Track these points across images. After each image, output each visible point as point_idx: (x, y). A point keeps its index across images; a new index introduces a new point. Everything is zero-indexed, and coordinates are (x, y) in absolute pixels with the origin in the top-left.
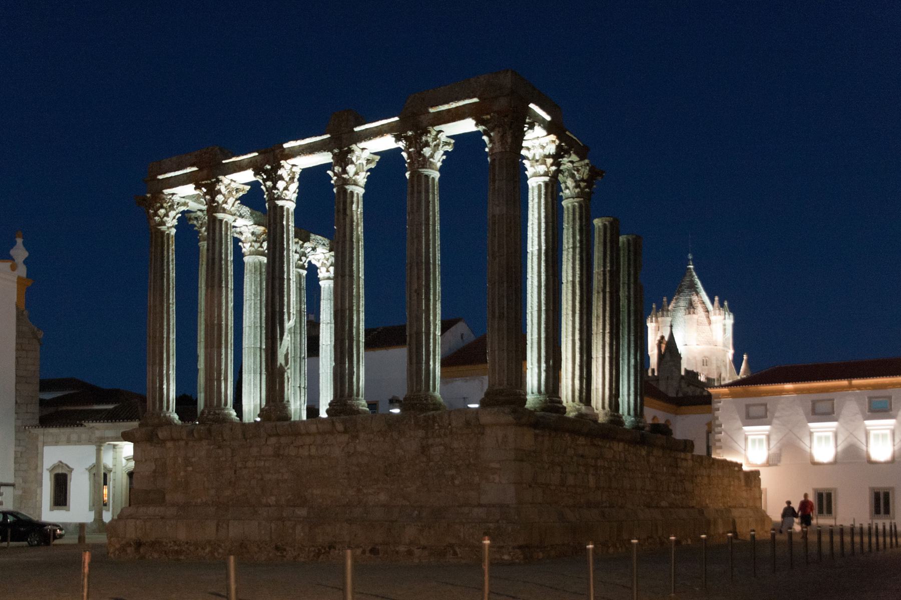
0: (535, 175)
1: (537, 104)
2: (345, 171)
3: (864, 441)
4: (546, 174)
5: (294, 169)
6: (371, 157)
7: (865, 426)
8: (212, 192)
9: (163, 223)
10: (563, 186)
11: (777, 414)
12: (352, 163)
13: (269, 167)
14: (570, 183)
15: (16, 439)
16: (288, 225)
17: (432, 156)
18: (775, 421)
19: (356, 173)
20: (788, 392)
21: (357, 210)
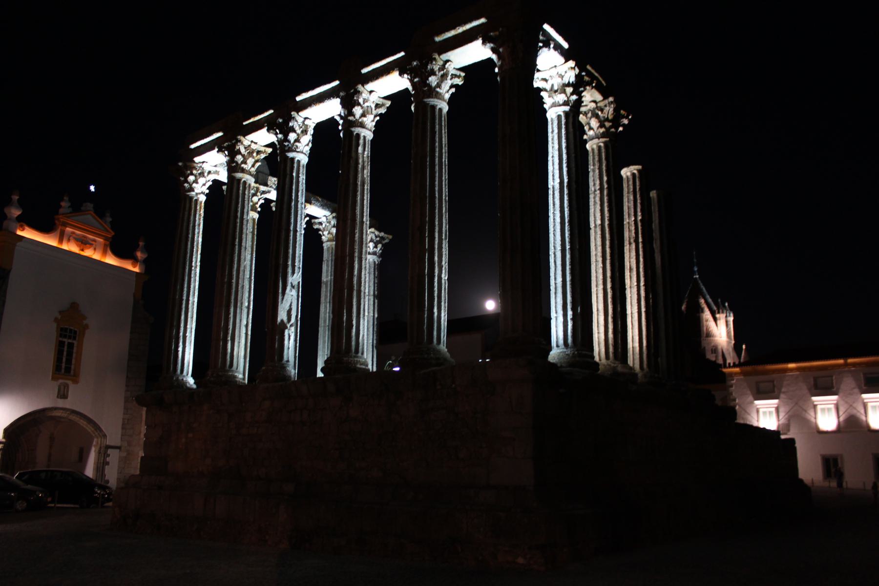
0: (554, 105)
1: (552, 26)
2: (351, 113)
3: (862, 411)
4: (566, 103)
5: (307, 122)
6: (380, 101)
7: (863, 399)
8: (233, 153)
9: (192, 190)
10: (586, 128)
11: (783, 390)
12: (359, 104)
13: (281, 121)
14: (594, 123)
15: (125, 408)
16: (298, 176)
17: (439, 85)
18: (782, 396)
19: (363, 115)
20: (792, 370)
21: (364, 153)
